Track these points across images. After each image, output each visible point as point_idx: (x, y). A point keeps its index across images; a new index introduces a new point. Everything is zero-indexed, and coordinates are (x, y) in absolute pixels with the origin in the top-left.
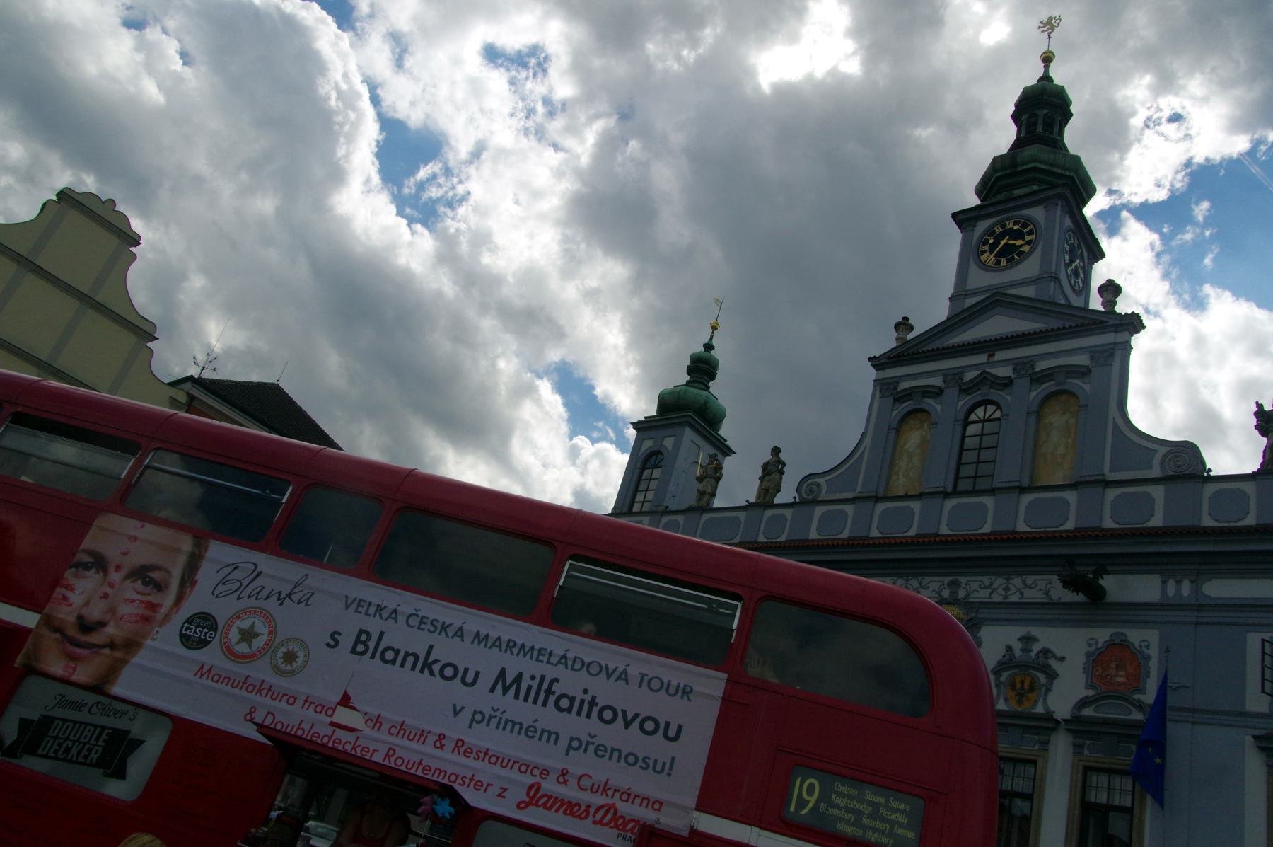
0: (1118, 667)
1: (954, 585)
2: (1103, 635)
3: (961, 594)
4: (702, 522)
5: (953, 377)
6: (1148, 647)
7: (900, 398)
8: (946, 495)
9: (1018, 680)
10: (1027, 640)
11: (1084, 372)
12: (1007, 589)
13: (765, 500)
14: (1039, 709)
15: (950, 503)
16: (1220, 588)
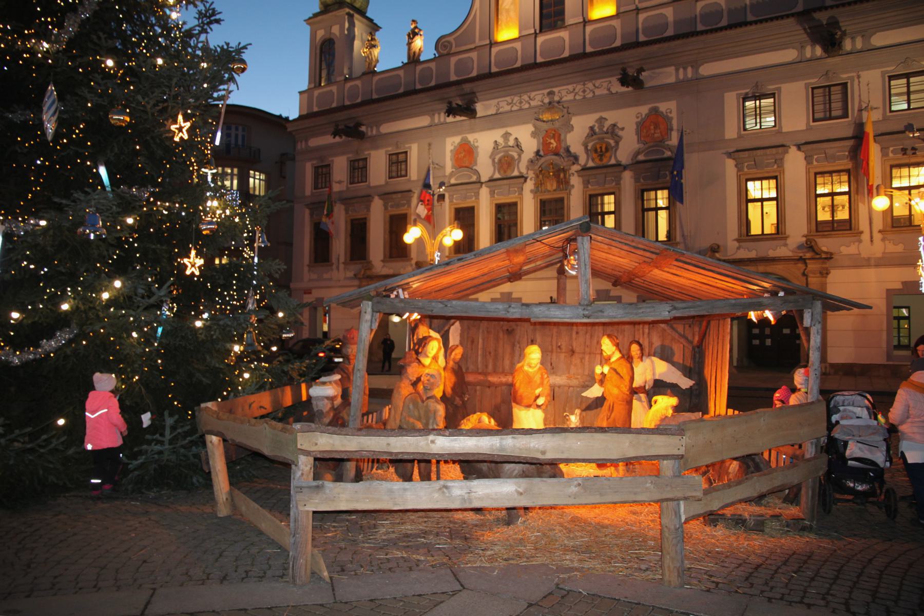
1: (551, 93)
2: (644, 110)
6: (671, 112)
9: (598, 146)
10: (601, 120)
12: (584, 91)
13: (414, 59)
14: (613, 162)
16: (707, 70)
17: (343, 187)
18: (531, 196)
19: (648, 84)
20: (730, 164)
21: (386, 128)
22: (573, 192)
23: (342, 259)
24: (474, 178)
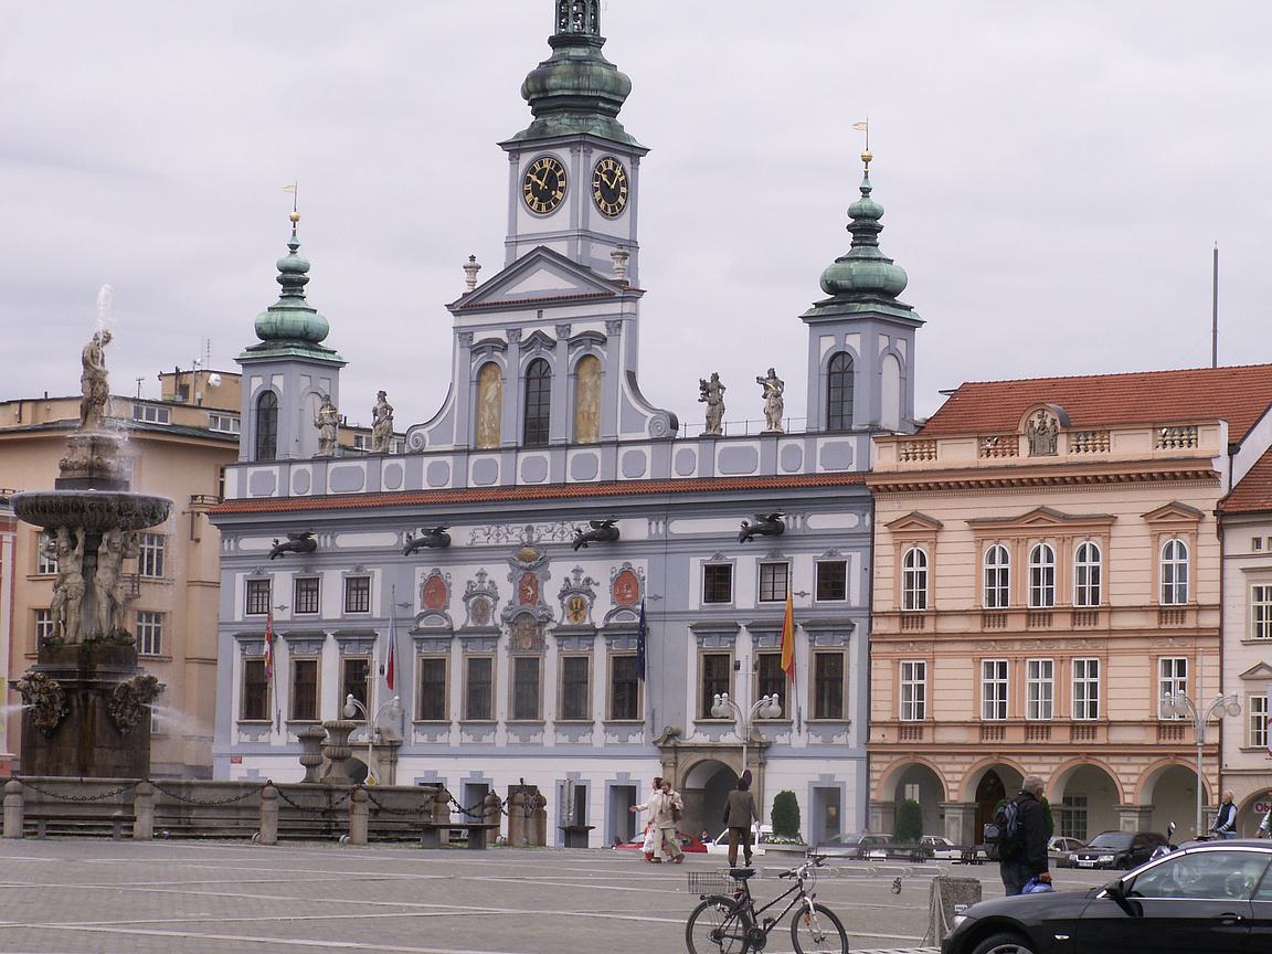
0: (628, 587)
1: (529, 529)
2: (619, 564)
3: (535, 537)
4: (329, 472)
5: (514, 332)
7: (476, 350)
8: (518, 449)
10: (577, 571)
11: (603, 341)
12: (563, 532)
14: (587, 622)
15: (523, 456)
16: (681, 527)
17: (286, 615)
18: (506, 653)
19: (623, 537)
20: (692, 644)
21: (346, 541)
22: (548, 652)
23: (284, 718)
24: (446, 624)
